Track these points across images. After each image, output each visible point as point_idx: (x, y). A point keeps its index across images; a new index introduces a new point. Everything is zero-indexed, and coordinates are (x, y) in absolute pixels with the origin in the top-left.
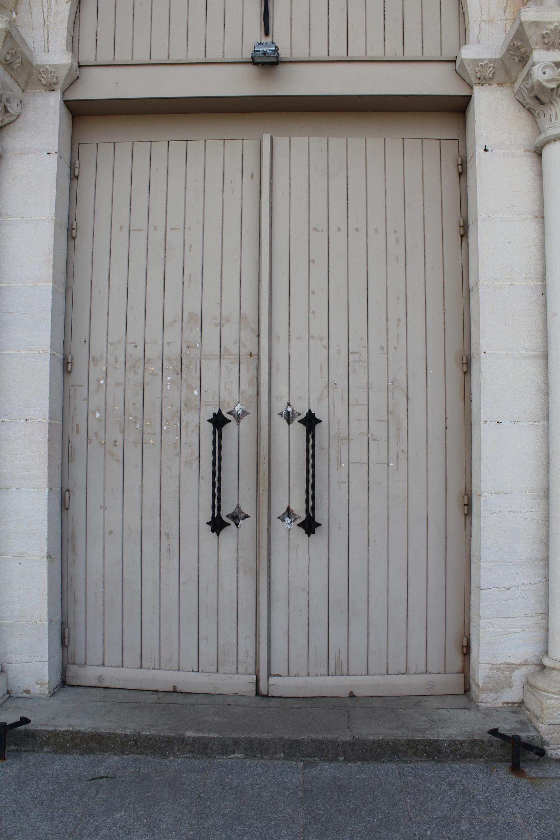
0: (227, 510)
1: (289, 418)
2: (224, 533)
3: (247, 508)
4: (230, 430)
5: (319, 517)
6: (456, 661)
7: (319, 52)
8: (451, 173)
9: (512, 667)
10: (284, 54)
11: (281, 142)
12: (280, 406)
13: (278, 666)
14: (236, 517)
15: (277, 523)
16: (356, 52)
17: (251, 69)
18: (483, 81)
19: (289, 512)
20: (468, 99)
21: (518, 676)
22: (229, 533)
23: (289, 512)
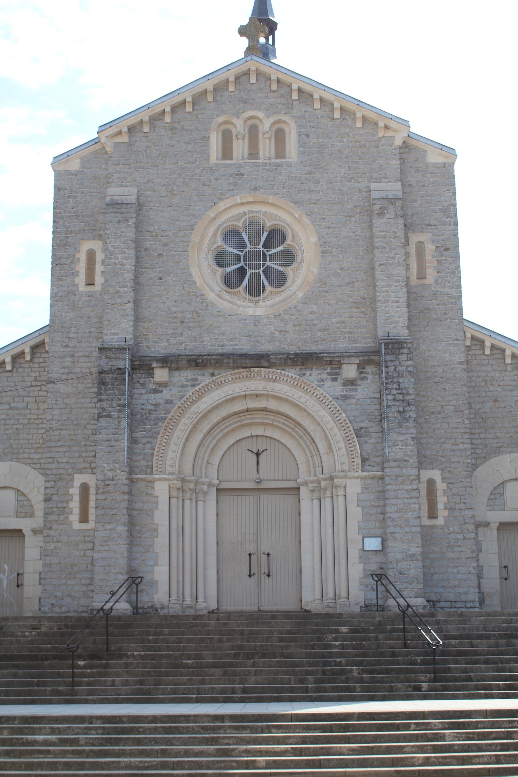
0: (252, 573)
1: (264, 554)
2: (251, 578)
3: (256, 572)
4: (252, 557)
5: (271, 574)
6: (299, 604)
7: (269, 478)
8: (298, 502)
9: (309, 602)
10: (262, 479)
11: (261, 496)
12: (262, 552)
13: (263, 604)
14: (254, 574)
15: (262, 575)
16: (277, 478)
17: (254, 482)
18: (302, 485)
19: (264, 573)
20: (299, 489)
21: (310, 603)
22: (252, 577)
23: (264, 573)
